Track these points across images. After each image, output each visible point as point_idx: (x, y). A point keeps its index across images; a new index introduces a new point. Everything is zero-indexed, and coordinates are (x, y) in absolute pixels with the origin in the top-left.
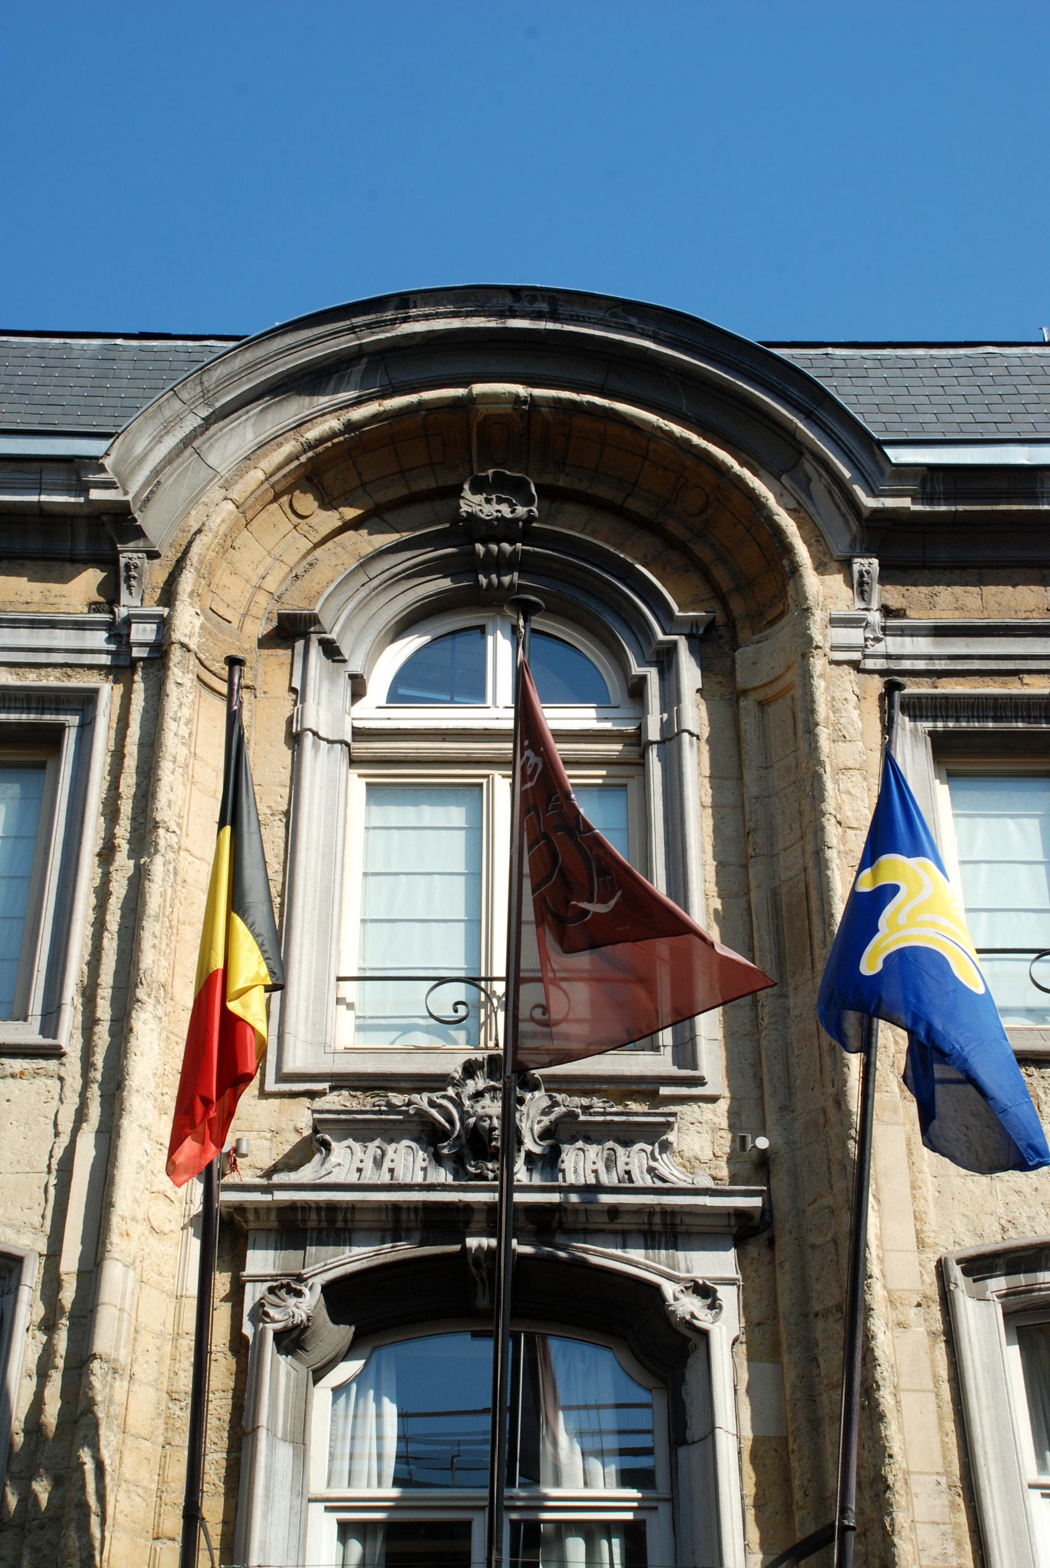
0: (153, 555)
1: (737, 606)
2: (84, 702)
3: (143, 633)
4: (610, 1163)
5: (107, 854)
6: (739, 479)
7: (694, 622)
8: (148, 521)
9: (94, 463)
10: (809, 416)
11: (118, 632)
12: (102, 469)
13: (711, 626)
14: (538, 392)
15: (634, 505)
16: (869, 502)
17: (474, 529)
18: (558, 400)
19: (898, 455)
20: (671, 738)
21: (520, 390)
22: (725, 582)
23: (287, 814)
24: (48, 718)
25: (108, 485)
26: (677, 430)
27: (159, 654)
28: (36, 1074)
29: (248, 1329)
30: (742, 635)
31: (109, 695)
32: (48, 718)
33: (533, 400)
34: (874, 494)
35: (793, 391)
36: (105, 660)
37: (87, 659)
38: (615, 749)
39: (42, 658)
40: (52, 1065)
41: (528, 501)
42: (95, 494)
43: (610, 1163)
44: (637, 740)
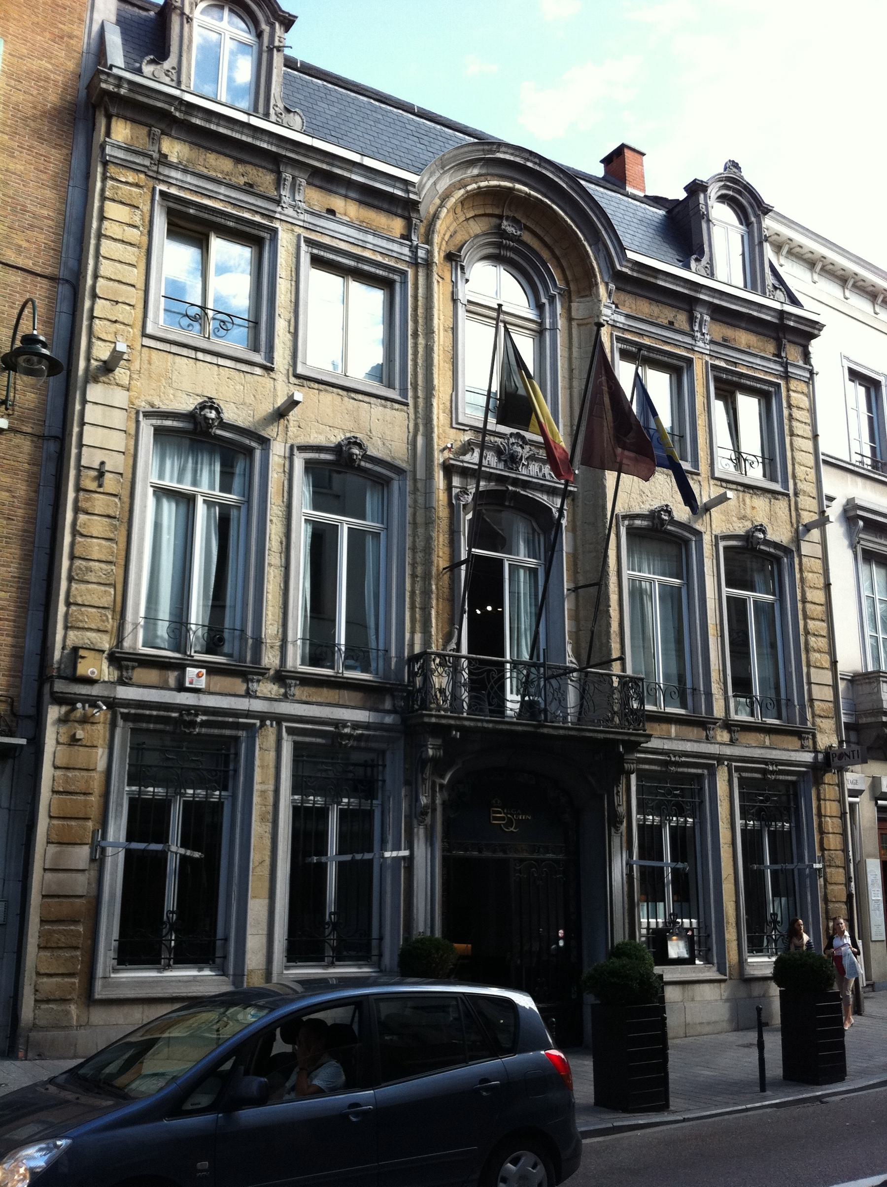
0: (421, 221)
1: (573, 287)
2: (404, 273)
3: (421, 253)
4: (540, 470)
5: (415, 335)
6: (584, 245)
7: (561, 289)
8: (422, 208)
9: (413, 184)
10: (606, 230)
11: (414, 249)
12: (414, 187)
13: (564, 290)
14: (532, 193)
15: (546, 239)
16: (619, 267)
17: (502, 234)
18: (537, 198)
19: (630, 255)
20: (554, 329)
21: (526, 189)
22: (570, 278)
23: (453, 328)
24: (391, 276)
25: (415, 193)
26: (569, 221)
27: (428, 264)
28: (402, 410)
29: (454, 502)
30: (573, 298)
31: (410, 273)
32: (391, 276)
33: (529, 195)
34: (621, 265)
35: (602, 220)
36: (407, 259)
37: (403, 257)
38: (533, 326)
39: (390, 253)
40: (405, 408)
41: (521, 230)
42: (412, 196)
43: (540, 470)
44: (541, 324)
